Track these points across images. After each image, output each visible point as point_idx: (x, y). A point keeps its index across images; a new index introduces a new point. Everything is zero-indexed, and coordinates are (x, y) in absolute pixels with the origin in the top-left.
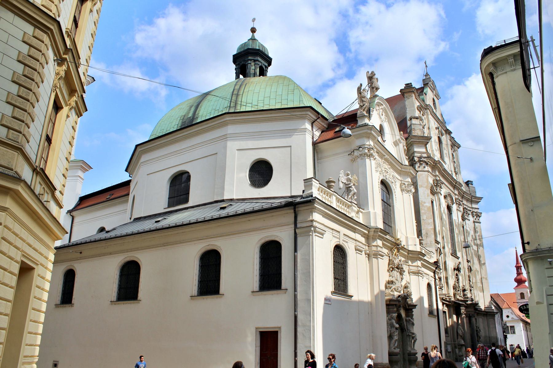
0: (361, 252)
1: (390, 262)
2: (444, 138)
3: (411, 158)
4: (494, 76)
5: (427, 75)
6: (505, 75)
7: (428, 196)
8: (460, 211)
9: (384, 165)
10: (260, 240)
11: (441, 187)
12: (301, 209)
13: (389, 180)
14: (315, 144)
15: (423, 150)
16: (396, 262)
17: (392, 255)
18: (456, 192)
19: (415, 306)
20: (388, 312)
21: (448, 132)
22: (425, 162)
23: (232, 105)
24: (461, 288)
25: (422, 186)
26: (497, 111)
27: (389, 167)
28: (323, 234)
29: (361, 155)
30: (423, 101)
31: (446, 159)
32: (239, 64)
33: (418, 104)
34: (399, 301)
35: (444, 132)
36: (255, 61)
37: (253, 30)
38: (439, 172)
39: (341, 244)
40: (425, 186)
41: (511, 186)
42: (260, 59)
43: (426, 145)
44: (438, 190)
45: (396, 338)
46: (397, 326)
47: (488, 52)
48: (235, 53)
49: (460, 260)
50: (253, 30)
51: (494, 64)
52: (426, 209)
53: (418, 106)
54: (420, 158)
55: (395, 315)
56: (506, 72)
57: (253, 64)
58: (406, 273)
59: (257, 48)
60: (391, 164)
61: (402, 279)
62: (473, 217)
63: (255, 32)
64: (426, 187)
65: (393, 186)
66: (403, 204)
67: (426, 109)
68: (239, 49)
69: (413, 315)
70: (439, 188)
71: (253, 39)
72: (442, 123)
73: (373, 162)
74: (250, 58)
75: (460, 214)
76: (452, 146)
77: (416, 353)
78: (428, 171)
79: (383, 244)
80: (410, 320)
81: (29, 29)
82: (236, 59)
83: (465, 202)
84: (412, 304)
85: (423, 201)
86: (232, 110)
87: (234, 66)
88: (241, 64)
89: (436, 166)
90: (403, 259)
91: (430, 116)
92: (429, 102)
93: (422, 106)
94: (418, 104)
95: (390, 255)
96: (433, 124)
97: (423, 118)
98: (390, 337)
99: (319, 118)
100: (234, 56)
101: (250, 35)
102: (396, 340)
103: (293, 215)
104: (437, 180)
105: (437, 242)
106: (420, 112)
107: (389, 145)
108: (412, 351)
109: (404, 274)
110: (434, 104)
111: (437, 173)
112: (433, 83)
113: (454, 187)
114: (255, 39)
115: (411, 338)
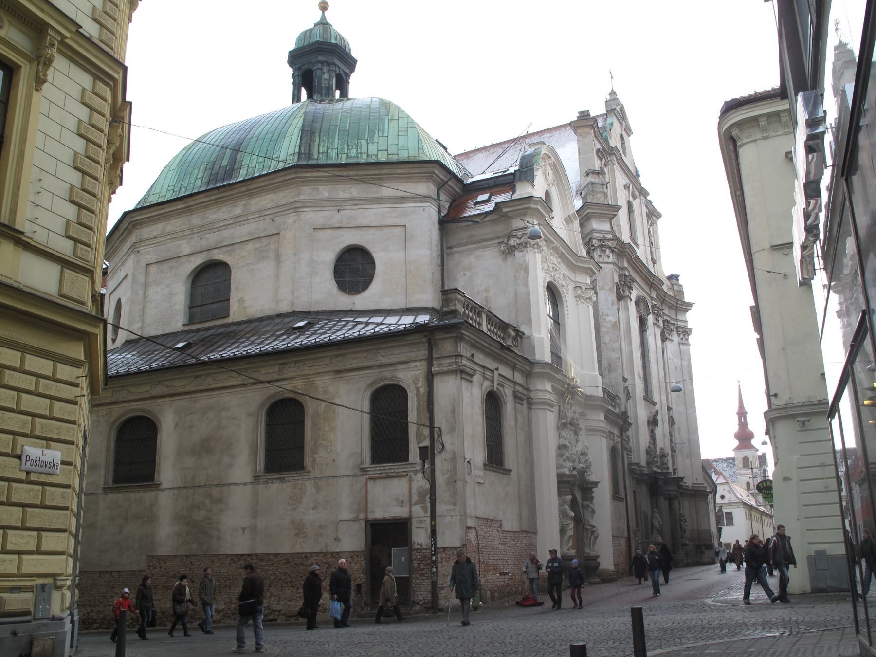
0: (522, 399)
1: (561, 415)
2: (636, 203)
3: (587, 240)
4: (738, 144)
5: (613, 93)
6: (753, 144)
7: (613, 304)
8: (659, 326)
9: (552, 258)
10: (372, 384)
11: (631, 288)
12: (438, 336)
13: (560, 282)
15: (606, 227)
16: (570, 414)
17: (564, 403)
18: (654, 295)
19: (596, 484)
20: (560, 494)
21: (643, 193)
22: (610, 248)
24: (658, 452)
25: (603, 288)
26: (738, 193)
27: (559, 260)
28: (472, 376)
29: (521, 244)
30: (606, 141)
31: (640, 241)
32: (300, 68)
33: (599, 146)
34: (574, 476)
35: (637, 193)
36: (329, 64)
37: (324, 7)
38: (628, 262)
40: (608, 288)
41: (754, 310)
42: (337, 62)
43: (611, 219)
44: (627, 293)
45: (571, 533)
46: (573, 514)
47: (731, 107)
48: (292, 47)
49: (657, 407)
50: (324, 7)
51: (739, 124)
52: (609, 325)
53: (598, 150)
54: (604, 239)
55: (569, 497)
56: (755, 140)
57: (325, 69)
58: (582, 432)
59: (333, 41)
60: (562, 256)
61: (577, 441)
62: (679, 335)
64: (610, 290)
65: (563, 292)
66: (578, 316)
67: (610, 155)
68: (299, 40)
69: (592, 498)
70: (627, 289)
71: (323, 24)
72: (633, 177)
73: (539, 256)
74: (321, 58)
75: (658, 332)
76: (648, 215)
77: (598, 557)
78: (613, 263)
79: (553, 388)
80: (588, 505)
81: (86, 80)
82: (295, 58)
83: (666, 311)
84: (592, 480)
85: (606, 311)
87: (290, 71)
89: (624, 252)
90: (579, 410)
91: (616, 167)
92: (615, 142)
93: (604, 149)
94: (599, 146)
95: (561, 405)
96: (621, 179)
97: (606, 170)
98: (563, 531)
100: (290, 52)
101: (317, 16)
102: (571, 536)
104: (625, 276)
105: (625, 380)
106: (601, 160)
107: (558, 224)
108: (592, 554)
109: (581, 433)
110: (623, 144)
111: (626, 265)
112: (622, 109)
113: (651, 285)
114: (328, 24)
115: (590, 533)
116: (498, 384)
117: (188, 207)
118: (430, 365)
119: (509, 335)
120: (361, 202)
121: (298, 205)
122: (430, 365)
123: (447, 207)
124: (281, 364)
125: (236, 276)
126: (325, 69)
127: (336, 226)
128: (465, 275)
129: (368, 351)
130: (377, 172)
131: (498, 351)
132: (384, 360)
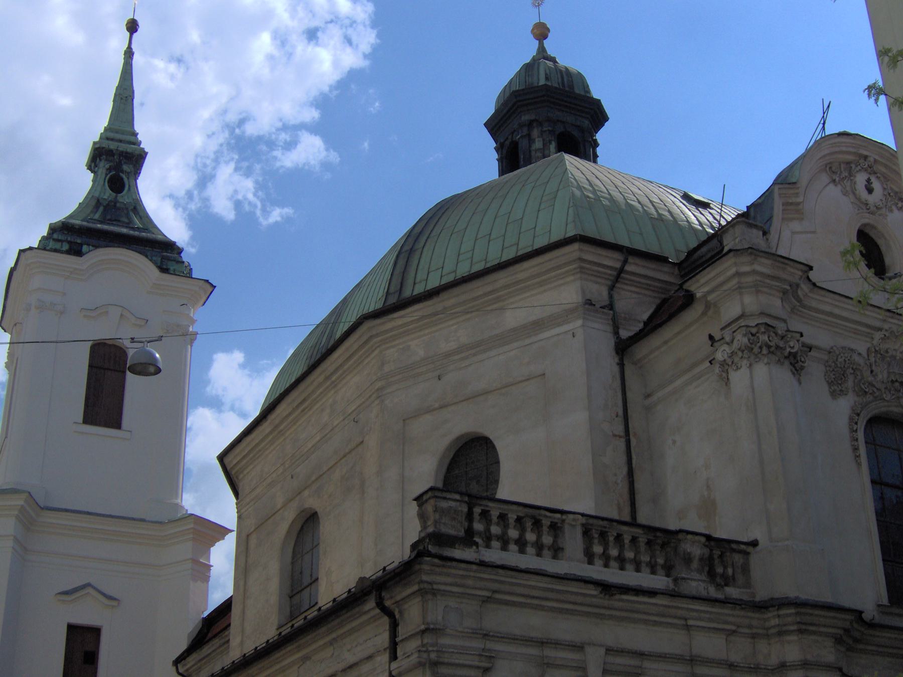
14: (623, 348)
23: (392, 289)
37: (541, 32)
50: (541, 32)
59: (542, 82)
63: (545, 38)
86: (392, 300)
88: (507, 143)
99: (625, 262)
101: (528, 51)
103: (386, 619)
117: (277, 427)
118: (394, 657)
120: (473, 351)
121: (379, 384)
122: (394, 657)
123: (645, 317)
125: (327, 528)
126: (535, 133)
127: (437, 405)
128: (674, 442)
129: (331, 643)
130: (489, 288)
131: (606, 603)
132: (351, 659)
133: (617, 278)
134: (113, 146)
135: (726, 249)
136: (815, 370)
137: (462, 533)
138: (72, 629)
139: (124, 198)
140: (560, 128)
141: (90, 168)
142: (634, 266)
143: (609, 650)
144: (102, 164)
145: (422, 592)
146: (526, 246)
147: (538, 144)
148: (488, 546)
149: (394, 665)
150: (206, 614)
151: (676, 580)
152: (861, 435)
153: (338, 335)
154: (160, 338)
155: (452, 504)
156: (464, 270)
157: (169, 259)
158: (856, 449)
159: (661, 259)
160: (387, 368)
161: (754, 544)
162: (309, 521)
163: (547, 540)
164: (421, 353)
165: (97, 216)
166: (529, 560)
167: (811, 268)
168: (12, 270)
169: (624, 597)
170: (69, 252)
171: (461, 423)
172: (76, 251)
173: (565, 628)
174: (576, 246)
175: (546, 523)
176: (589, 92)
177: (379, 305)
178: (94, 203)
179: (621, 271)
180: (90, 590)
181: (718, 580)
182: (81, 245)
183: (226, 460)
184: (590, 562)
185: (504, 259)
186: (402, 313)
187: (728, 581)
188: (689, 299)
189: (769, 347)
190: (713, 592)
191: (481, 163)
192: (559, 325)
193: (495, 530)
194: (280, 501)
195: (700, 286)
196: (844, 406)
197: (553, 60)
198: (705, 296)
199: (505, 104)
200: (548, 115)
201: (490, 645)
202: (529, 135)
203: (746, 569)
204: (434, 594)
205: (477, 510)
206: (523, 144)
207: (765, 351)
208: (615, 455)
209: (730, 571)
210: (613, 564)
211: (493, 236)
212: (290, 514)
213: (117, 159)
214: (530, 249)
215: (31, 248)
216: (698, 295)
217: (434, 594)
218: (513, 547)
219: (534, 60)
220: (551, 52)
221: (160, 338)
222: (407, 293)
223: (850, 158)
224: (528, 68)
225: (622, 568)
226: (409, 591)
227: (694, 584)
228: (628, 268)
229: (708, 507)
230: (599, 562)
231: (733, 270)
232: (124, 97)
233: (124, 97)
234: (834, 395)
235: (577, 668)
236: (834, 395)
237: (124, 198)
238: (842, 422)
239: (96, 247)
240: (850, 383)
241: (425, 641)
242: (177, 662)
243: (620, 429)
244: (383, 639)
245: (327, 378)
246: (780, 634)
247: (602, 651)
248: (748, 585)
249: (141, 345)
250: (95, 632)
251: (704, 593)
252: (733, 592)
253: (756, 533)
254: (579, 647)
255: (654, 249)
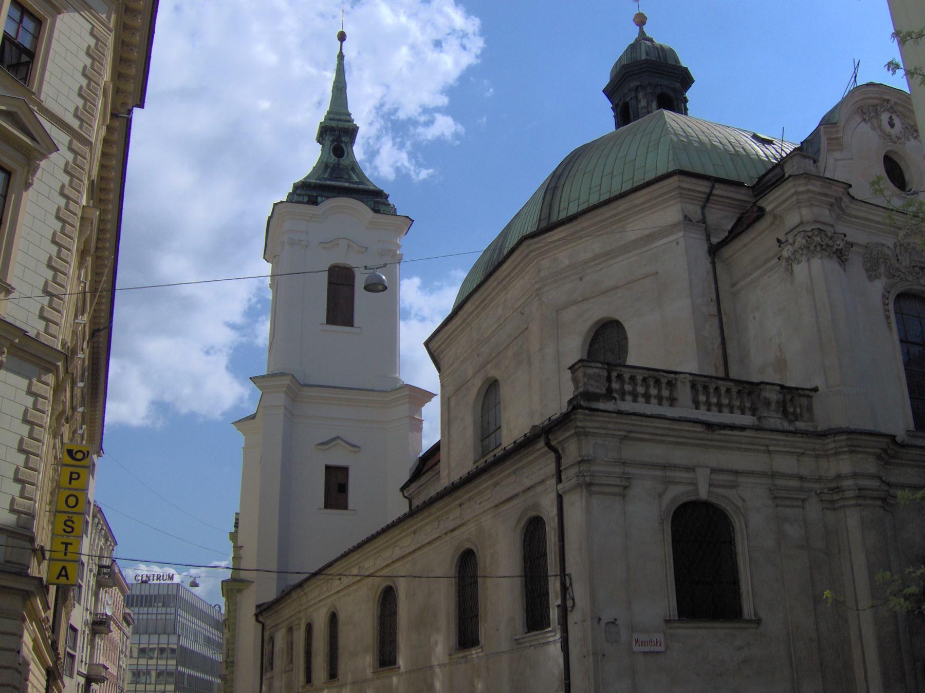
10: (519, 520)
14: (714, 251)
23: (543, 217)
37: (641, 20)
39: (703, 494)
50: (641, 20)
59: (644, 57)
63: (644, 24)
86: (544, 224)
88: (621, 103)
99: (713, 187)
101: (633, 34)
116: (710, 485)
117: (465, 320)
118: (559, 480)
119: (768, 403)
121: (537, 286)
122: (559, 480)
123: (729, 228)
124: (460, 505)
125: (505, 391)
126: (641, 95)
127: (580, 299)
128: (754, 318)
129: (514, 472)
130: (614, 212)
131: (710, 437)
132: (528, 483)
133: (708, 200)
134: (334, 124)
135: (787, 176)
136: (856, 260)
137: (604, 391)
138: (328, 468)
139: (344, 161)
140: (658, 91)
141: (319, 141)
142: (720, 190)
143: (713, 471)
144: (327, 138)
145: (577, 434)
146: (639, 180)
147: (643, 103)
148: (623, 400)
149: (560, 486)
150: (421, 454)
151: (759, 418)
152: (891, 307)
153: (506, 252)
154: (385, 265)
155: (596, 370)
156: (594, 199)
157: (379, 203)
158: (888, 318)
159: (739, 184)
160: (542, 274)
161: (815, 390)
162: (492, 387)
163: (665, 393)
164: (567, 262)
165: (326, 175)
166: (653, 408)
167: (850, 186)
168: (270, 219)
169: (722, 432)
170: (308, 203)
171: (598, 311)
172: (313, 202)
173: (681, 456)
174: (676, 178)
175: (664, 381)
176: (676, 60)
177: (534, 229)
178: (323, 166)
179: (710, 194)
180: (339, 441)
181: (791, 417)
182: (317, 197)
183: (430, 346)
184: (697, 408)
185: (623, 190)
186: (551, 233)
187: (797, 418)
188: (761, 212)
189: (821, 245)
190: (786, 426)
191: (601, 120)
192: (667, 236)
193: (628, 387)
194: (470, 372)
195: (769, 203)
196: (878, 286)
197: (651, 40)
198: (773, 210)
199: (616, 75)
200: (649, 82)
201: (628, 470)
202: (636, 97)
203: (810, 409)
204: (586, 436)
205: (614, 374)
206: (632, 104)
207: (819, 249)
208: (711, 329)
209: (798, 410)
210: (714, 408)
211: (615, 173)
212: (478, 382)
213: (337, 133)
214: (642, 182)
215: (282, 202)
216: (768, 209)
217: (586, 436)
218: (641, 399)
219: (637, 41)
220: (649, 34)
221: (385, 265)
222: (554, 218)
223: (876, 102)
224: (633, 48)
225: (720, 411)
226: (568, 434)
227: (772, 420)
228: (715, 192)
229: (781, 364)
230: (703, 408)
231: (793, 191)
232: (340, 88)
233: (340, 88)
234: (871, 278)
235: (691, 484)
236: (871, 278)
237: (344, 161)
238: (877, 300)
239: (328, 198)
240: (882, 269)
241: (582, 469)
242: (403, 489)
243: (714, 310)
244: (552, 468)
245: (500, 283)
246: (836, 454)
247: (708, 471)
248: (812, 419)
249: (371, 271)
250: (344, 470)
251: (780, 427)
252: (800, 425)
253: (817, 382)
254: (691, 469)
255: (733, 177)
